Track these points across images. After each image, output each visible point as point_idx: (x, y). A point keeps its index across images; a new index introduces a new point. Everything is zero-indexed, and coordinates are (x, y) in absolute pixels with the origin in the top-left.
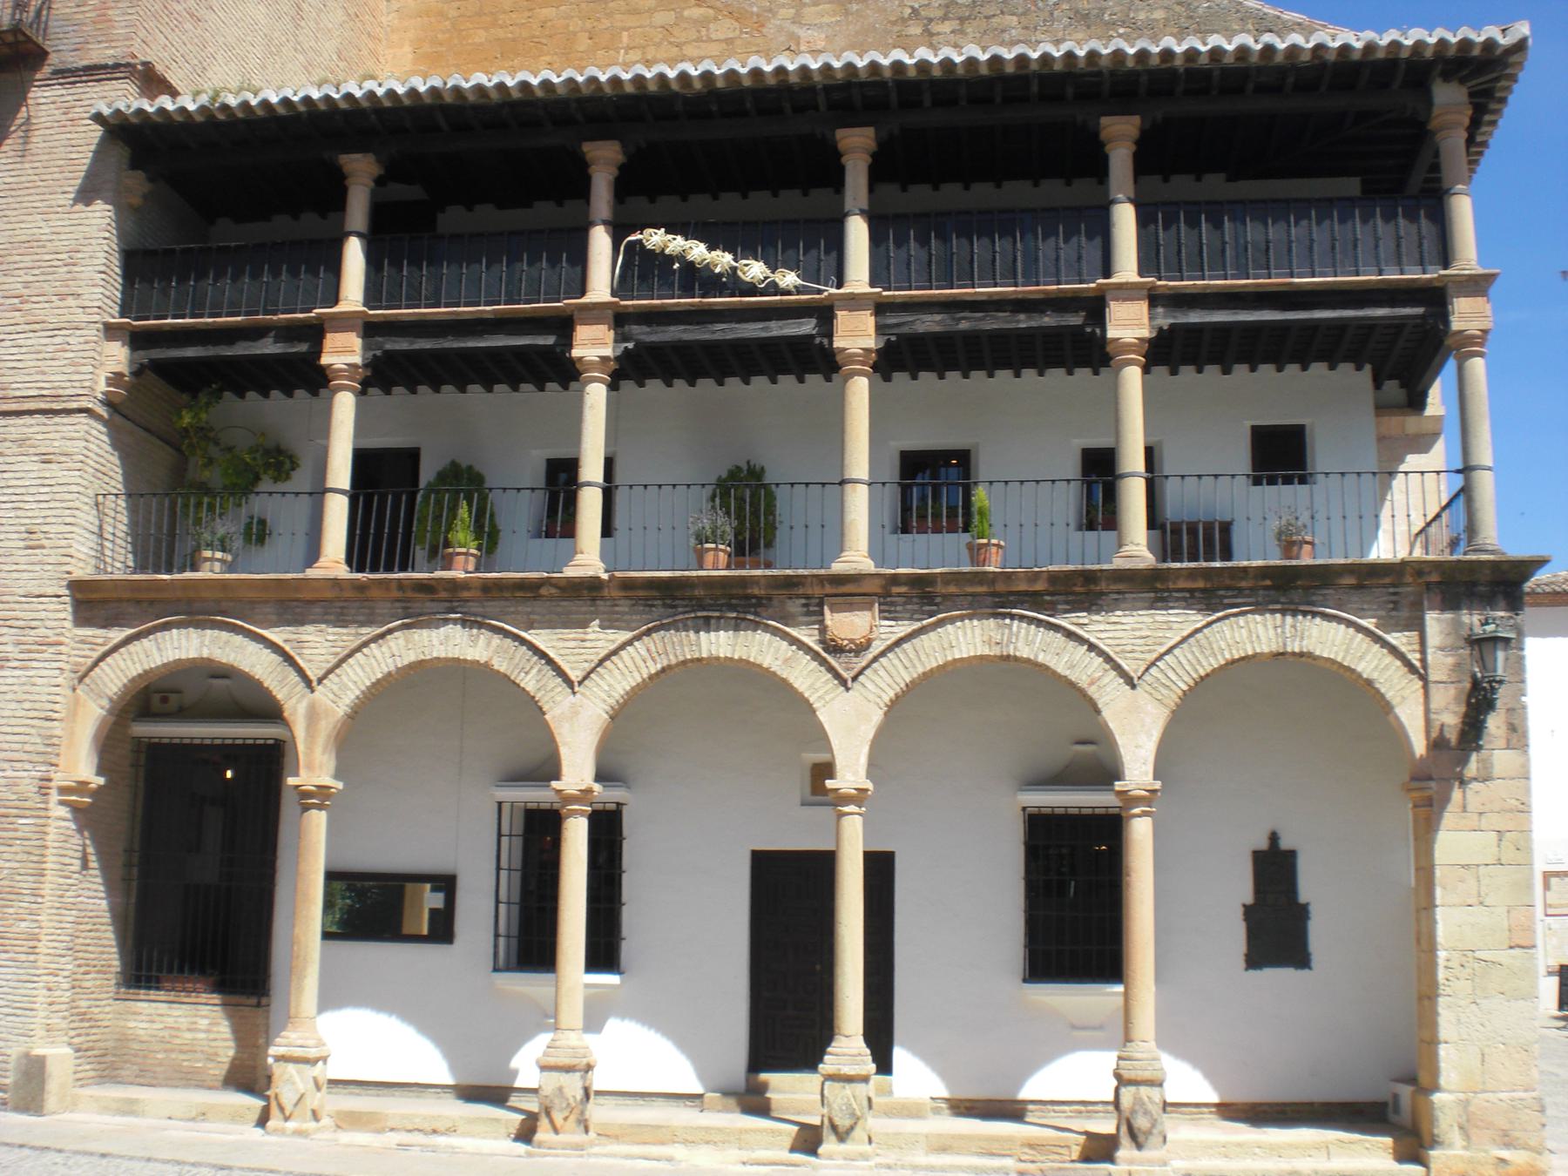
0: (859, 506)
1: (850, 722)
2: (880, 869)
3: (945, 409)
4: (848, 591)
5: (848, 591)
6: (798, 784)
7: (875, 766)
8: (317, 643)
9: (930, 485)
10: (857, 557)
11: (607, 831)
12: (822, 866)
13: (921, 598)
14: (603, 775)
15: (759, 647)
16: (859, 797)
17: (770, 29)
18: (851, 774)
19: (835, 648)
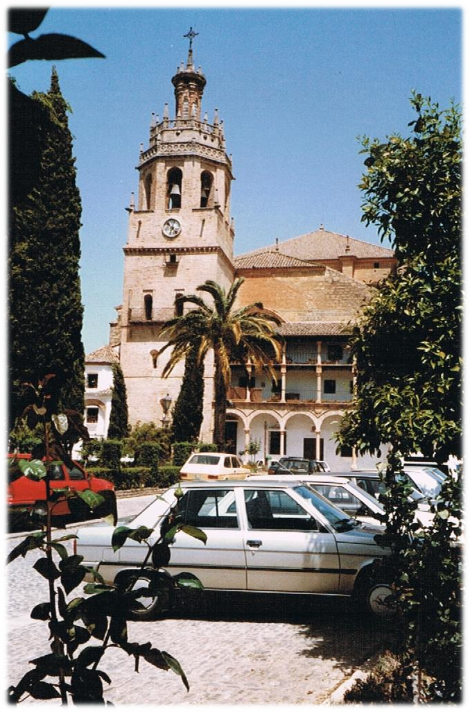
0: (319, 394)
1: (318, 423)
2: (322, 441)
3: (331, 376)
4: (318, 406)
5: (318, 406)
6: (311, 429)
7: (321, 429)
8: (247, 411)
9: (329, 387)
10: (319, 401)
11: (285, 434)
12: (314, 440)
13: (328, 407)
14: (285, 428)
15: (308, 414)
16: (319, 433)
17: (303, 295)
18: (318, 430)
19: (317, 413)
